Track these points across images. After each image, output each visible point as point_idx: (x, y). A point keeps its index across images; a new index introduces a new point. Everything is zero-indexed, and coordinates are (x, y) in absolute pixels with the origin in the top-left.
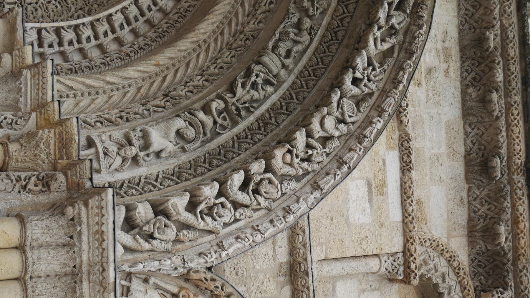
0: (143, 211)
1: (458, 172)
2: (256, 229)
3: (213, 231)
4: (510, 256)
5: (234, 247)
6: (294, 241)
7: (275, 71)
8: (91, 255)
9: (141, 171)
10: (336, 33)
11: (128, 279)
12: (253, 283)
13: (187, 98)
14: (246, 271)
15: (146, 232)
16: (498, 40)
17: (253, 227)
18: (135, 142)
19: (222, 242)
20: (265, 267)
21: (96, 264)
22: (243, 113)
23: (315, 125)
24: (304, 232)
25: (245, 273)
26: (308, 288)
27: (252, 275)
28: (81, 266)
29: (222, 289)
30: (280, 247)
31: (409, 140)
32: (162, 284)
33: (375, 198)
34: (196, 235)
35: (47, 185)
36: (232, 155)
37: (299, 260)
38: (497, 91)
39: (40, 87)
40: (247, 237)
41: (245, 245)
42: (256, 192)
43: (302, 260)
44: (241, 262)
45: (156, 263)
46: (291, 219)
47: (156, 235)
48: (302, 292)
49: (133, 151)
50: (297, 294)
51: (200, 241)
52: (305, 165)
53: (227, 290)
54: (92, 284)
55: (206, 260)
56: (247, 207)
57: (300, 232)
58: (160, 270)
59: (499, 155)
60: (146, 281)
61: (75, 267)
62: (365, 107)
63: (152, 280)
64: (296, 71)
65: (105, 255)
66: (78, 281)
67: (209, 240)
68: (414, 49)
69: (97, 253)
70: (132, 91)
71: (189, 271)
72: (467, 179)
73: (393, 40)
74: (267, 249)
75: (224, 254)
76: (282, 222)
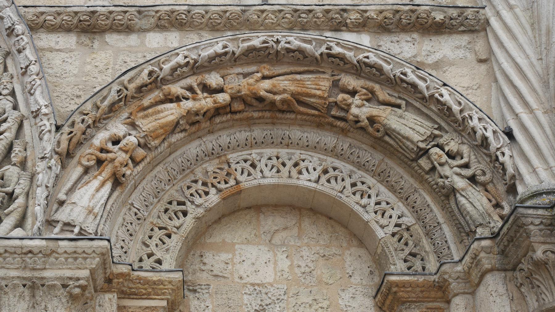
2: (25, 72)
3: (19, 122)
5: (40, 99)
6: (52, 25)
8: (12, 267)
11: (54, 224)
12: (94, 78)
14: (78, 85)
15: (5, 201)
17: (24, 74)
19: (32, 112)
20: (77, 63)
21: (24, 261)
24: (42, 13)
25: (80, 87)
26: (111, 12)
27: (84, 79)
28: (24, 278)
29: (87, 114)
30: (57, 43)
32: (69, 185)
34: (18, 143)
37: (75, 21)
40: (31, 82)
41: (40, 85)
43: (77, 18)
44: (66, 90)
46: (19, 28)
47: (9, 189)
48: (114, 20)
50: (117, 26)
51: (28, 138)
53: (88, 109)
54: (47, 267)
55: (46, 132)
57: (42, 18)
58: (47, 187)
60: (61, 203)
61: (24, 286)
63: (62, 196)
65: (13, 250)
66: (42, 283)
67: (29, 127)
69: (11, 259)
71: (57, 153)
74: (56, 59)
75: (44, 110)
76: (22, 38)
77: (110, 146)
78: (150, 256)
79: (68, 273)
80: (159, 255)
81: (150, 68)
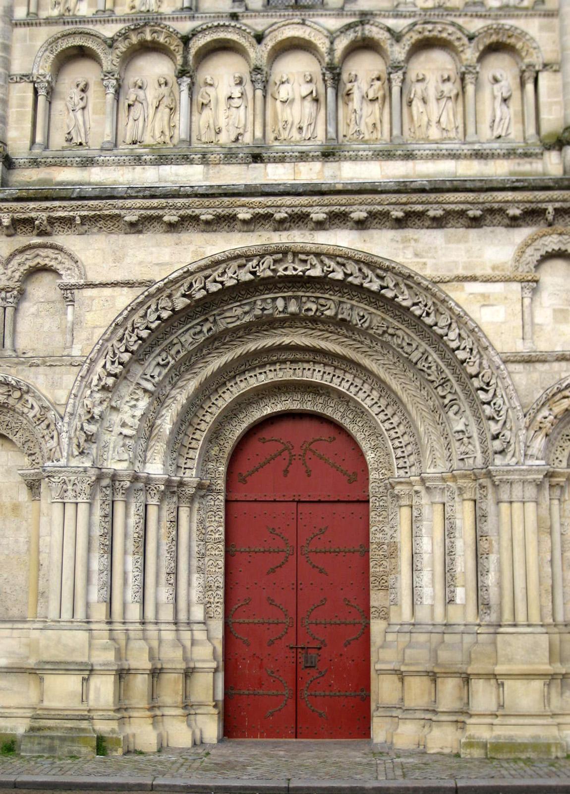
0: (497, 445)
1: (475, 234)
4: (527, 205)
7: (421, 355)
9: (475, 435)
10: (396, 315)
13: (434, 401)
16: (397, 207)
18: (461, 436)
22: (444, 377)
23: (454, 345)
31: (458, 277)
33: (491, 302)
35: (484, 487)
36: (467, 388)
38: (428, 210)
39: (433, 479)
42: (488, 384)
45: (521, 444)
47: (508, 440)
49: (465, 440)
52: (474, 352)
56: (495, 390)
59: (467, 210)
62: (441, 310)
63: (528, 444)
64: (420, 341)
68: (408, 274)
70: (431, 429)
72: (481, 227)
73: (402, 286)
74: (517, 377)
77: (543, 420)
78: (557, 458)
79: (535, 476)
80: (560, 458)
81: (558, 386)
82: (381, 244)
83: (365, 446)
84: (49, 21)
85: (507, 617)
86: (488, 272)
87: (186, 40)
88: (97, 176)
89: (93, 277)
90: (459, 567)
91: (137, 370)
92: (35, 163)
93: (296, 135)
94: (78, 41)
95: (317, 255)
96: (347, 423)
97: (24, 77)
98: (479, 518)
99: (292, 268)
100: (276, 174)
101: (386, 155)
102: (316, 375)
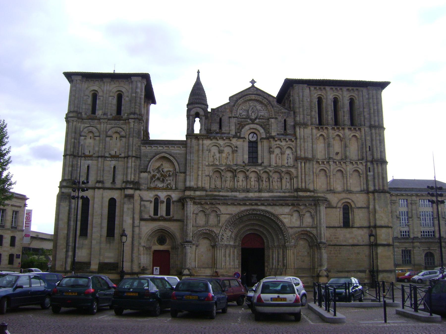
82: (269, 209)
83: (264, 239)
84: (212, 165)
85: (288, 267)
86: (285, 213)
87: (235, 170)
88: (221, 194)
89: (222, 212)
90: (280, 260)
91: (229, 228)
92: (211, 191)
93: (253, 187)
94: (217, 170)
95: (259, 210)
96: (261, 235)
97: (209, 176)
98: (283, 252)
99: (255, 212)
100: (251, 195)
101: (269, 192)
102: (257, 228)
